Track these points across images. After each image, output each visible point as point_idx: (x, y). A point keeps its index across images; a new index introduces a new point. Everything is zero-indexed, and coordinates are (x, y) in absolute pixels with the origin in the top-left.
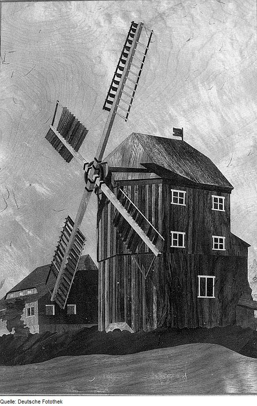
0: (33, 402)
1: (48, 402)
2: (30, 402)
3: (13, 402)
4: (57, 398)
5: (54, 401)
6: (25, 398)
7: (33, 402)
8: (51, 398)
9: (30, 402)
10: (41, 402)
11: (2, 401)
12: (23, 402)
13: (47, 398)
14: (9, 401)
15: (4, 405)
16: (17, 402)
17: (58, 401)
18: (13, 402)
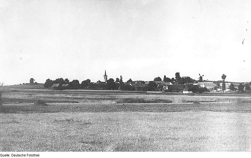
0: (21, 156)
1: (31, 155)
2: (19, 156)
3: (8, 155)
4: (36, 153)
5: (34, 155)
6: (16, 153)
7: (21, 156)
8: (32, 153)
9: (19, 156)
10: (26, 155)
11: (1, 155)
12: (14, 155)
13: (29, 153)
14: (5, 155)
15: (3, 157)
16: (11, 155)
17: (37, 155)
18: (8, 155)
